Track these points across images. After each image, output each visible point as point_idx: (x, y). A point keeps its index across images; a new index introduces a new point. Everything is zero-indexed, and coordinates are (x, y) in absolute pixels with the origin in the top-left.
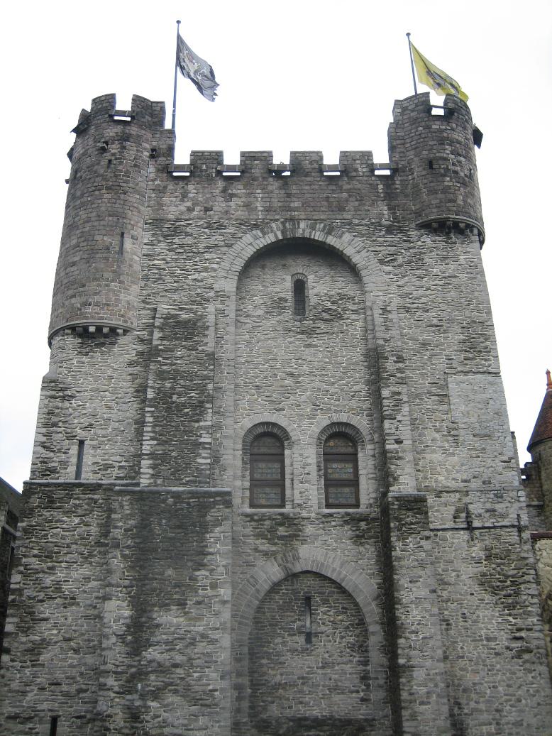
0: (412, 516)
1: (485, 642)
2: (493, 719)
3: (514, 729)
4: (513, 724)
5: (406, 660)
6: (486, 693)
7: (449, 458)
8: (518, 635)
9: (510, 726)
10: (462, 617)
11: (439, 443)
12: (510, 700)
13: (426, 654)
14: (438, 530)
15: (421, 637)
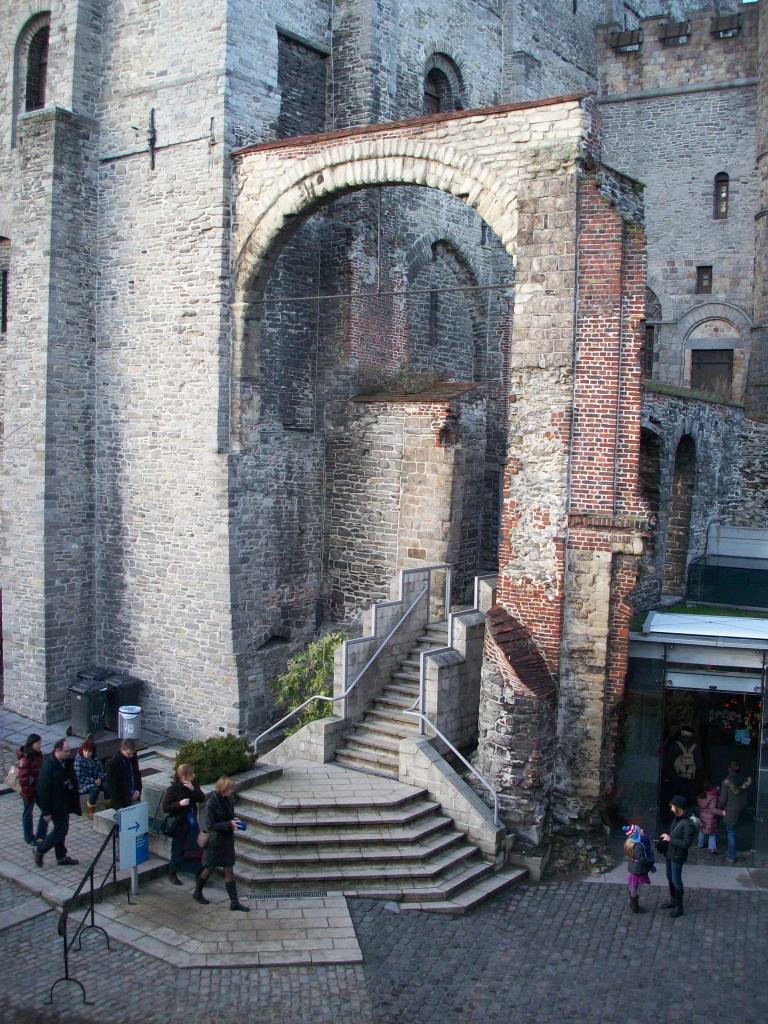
0: (38, 145)
1: (152, 322)
2: (150, 428)
3: (170, 442)
4: (170, 435)
5: (12, 350)
6: (144, 394)
7: (146, 40)
8: (189, 310)
9: (166, 437)
10: (130, 288)
11: (137, 18)
12: (169, 403)
13: (31, 341)
14: (119, 158)
15: (30, 317)
